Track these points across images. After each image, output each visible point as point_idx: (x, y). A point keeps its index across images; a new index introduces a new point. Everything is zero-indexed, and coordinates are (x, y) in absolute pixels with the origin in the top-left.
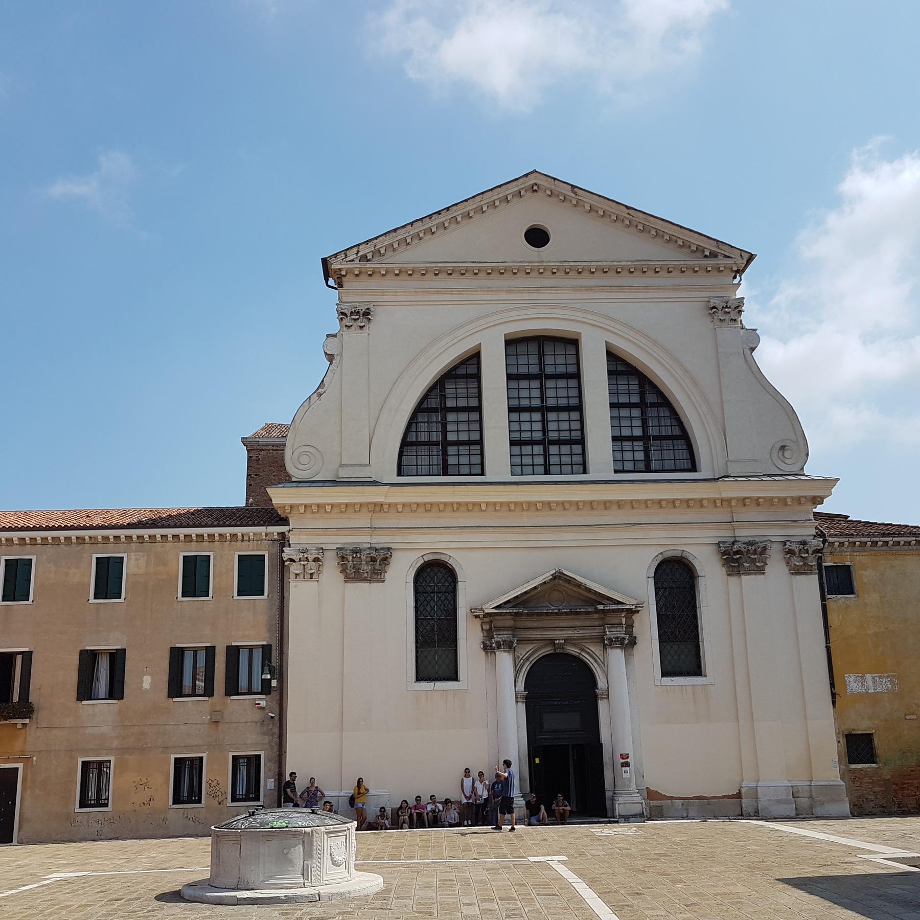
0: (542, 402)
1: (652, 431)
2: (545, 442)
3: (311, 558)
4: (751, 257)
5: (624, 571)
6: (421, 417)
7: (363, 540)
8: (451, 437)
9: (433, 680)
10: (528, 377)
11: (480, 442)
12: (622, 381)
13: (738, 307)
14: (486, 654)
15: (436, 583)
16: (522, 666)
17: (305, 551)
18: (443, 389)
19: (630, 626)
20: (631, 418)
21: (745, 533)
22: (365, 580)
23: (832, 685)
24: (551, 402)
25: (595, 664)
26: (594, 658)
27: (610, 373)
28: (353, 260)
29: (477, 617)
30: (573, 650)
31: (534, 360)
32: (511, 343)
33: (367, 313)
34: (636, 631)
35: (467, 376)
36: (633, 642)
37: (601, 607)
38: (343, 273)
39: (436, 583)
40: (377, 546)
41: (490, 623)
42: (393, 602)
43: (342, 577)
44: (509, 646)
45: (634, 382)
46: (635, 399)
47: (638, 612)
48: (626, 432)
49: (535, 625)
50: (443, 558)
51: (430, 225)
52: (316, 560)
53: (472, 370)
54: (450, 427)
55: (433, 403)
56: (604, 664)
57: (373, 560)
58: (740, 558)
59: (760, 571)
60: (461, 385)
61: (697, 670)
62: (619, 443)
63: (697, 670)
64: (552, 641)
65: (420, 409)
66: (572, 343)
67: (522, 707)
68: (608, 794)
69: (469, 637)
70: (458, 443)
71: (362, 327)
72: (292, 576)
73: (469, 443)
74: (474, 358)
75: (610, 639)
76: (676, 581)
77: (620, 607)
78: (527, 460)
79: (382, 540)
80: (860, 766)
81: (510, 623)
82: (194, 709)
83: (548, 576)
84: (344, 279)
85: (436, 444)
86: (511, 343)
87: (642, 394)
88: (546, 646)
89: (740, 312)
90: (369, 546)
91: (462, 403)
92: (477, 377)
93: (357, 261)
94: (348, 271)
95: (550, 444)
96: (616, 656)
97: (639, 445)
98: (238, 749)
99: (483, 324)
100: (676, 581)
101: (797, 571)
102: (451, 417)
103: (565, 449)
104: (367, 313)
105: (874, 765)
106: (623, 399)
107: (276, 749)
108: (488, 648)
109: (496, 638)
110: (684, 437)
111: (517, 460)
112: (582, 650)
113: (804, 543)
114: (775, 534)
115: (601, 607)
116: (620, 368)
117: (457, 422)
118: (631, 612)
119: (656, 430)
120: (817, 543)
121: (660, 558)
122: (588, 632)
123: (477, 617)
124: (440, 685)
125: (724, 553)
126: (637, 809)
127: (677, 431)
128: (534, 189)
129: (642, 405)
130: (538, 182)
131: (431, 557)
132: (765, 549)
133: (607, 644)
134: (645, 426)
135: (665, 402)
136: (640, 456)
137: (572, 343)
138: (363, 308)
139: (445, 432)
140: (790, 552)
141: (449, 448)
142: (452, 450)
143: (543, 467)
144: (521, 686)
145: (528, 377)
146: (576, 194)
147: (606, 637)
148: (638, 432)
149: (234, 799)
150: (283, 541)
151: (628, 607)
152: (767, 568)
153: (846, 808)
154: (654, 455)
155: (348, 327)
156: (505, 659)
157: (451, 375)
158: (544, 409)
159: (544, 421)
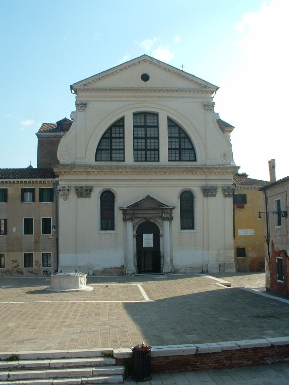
0: (145, 136)
1: (182, 147)
2: (146, 150)
3: (66, 189)
4: (218, 88)
5: (170, 196)
6: (104, 140)
7: (84, 184)
8: (114, 147)
9: (107, 230)
10: (141, 127)
11: (124, 149)
12: (173, 129)
13: (213, 105)
14: (124, 222)
15: (108, 198)
16: (136, 226)
17: (64, 187)
18: (111, 131)
19: (171, 213)
20: (175, 142)
21: (210, 183)
22: (84, 197)
23: (234, 233)
24: (148, 136)
25: (160, 226)
26: (159, 224)
27: (168, 126)
28: (81, 86)
29: (121, 210)
30: (152, 221)
31: (143, 121)
32: (135, 114)
33: (85, 105)
34: (173, 215)
35: (119, 126)
36: (172, 219)
37: (162, 207)
38: (77, 90)
39: (108, 198)
40: (88, 186)
41: (125, 212)
42: (93, 203)
43: (76, 196)
44: (131, 219)
45: (177, 129)
46: (177, 135)
47: (174, 209)
48: (173, 147)
49: (140, 212)
50: (110, 190)
51: (108, 73)
52: (68, 190)
53: (121, 124)
54: (114, 144)
55: (108, 135)
56: (162, 225)
57: (87, 190)
58: (208, 192)
59: (214, 196)
60: (118, 129)
61: (192, 227)
62: (171, 151)
63: (192, 227)
64: (145, 218)
65: (103, 137)
66: (156, 115)
67: (135, 239)
68: (162, 266)
69: (118, 216)
70: (116, 150)
71: (84, 109)
72: (60, 196)
73: (120, 149)
74: (122, 119)
75: (164, 218)
76: (187, 200)
77: (168, 207)
78: (139, 156)
79: (89, 184)
80: (240, 258)
81: (132, 212)
82: (30, 238)
83: (145, 196)
84: (77, 92)
85: (108, 150)
86: (135, 114)
87: (179, 134)
88: (143, 219)
89: (213, 107)
90: (85, 185)
91: (118, 135)
92: (123, 126)
93: (82, 86)
94: (79, 89)
95: (147, 151)
96: (166, 223)
97: (177, 151)
98: (44, 251)
99: (126, 109)
100: (187, 200)
101: (226, 196)
102: (114, 140)
103: (153, 152)
104: (85, 105)
105: (244, 257)
106: (173, 135)
107: (56, 251)
108: (124, 220)
109: (127, 217)
110: (193, 149)
111: (136, 156)
112: (155, 221)
113: (229, 187)
114: (220, 184)
115: (162, 207)
116: (173, 124)
117: (116, 142)
118: (172, 209)
119: (183, 146)
120: (233, 187)
121: (182, 191)
122: (158, 215)
123: (121, 210)
124: (109, 232)
125: (203, 190)
126: (170, 270)
127: (191, 147)
128: (144, 61)
129: (179, 138)
130: (146, 58)
131: (106, 190)
132: (216, 189)
133: (164, 219)
134: (180, 145)
135: (187, 137)
136: (178, 155)
137: (156, 115)
138: (84, 102)
139: (111, 145)
140: (224, 190)
141: (113, 151)
142: (114, 152)
143: (145, 158)
144: (135, 233)
145: (141, 127)
146: (159, 63)
147: (163, 217)
148: (177, 147)
149: (43, 266)
150: (56, 183)
151: (170, 207)
152: (217, 195)
153: (234, 270)
154: (183, 155)
155: (79, 109)
156: (130, 225)
157: (114, 125)
158: (146, 138)
159: (146, 143)
